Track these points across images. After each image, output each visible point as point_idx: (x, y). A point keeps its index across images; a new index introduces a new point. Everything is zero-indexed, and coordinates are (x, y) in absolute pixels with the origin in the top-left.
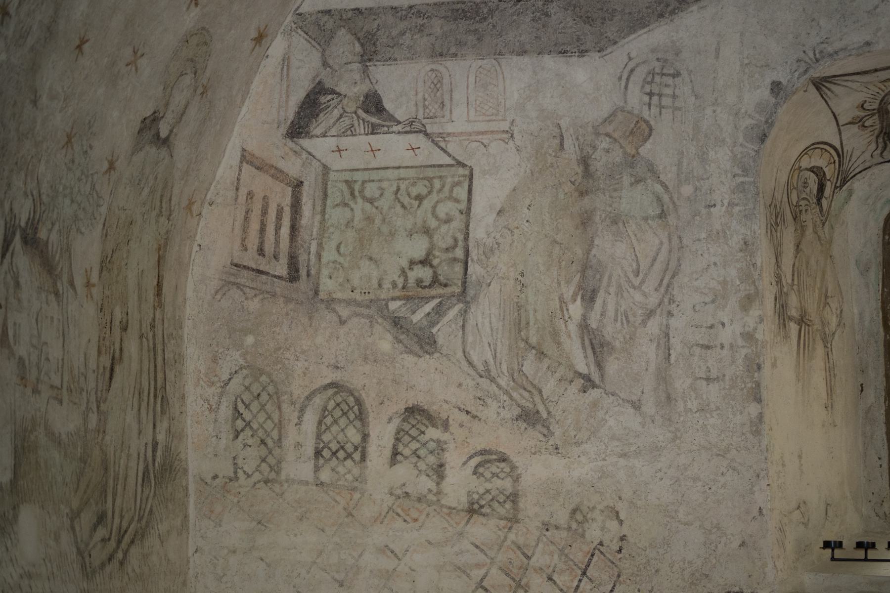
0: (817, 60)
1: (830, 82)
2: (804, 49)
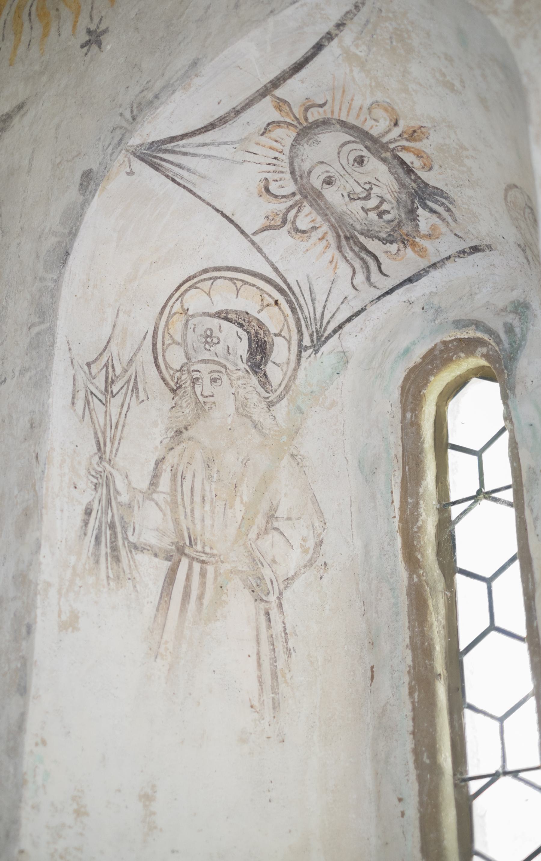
0: (134, 119)
1: (166, 151)
2: (121, 110)
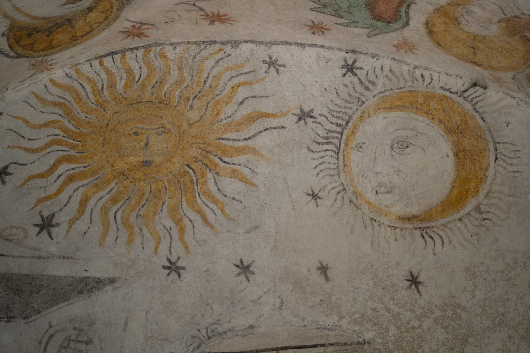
0: (209, 338)
2: (199, 328)
